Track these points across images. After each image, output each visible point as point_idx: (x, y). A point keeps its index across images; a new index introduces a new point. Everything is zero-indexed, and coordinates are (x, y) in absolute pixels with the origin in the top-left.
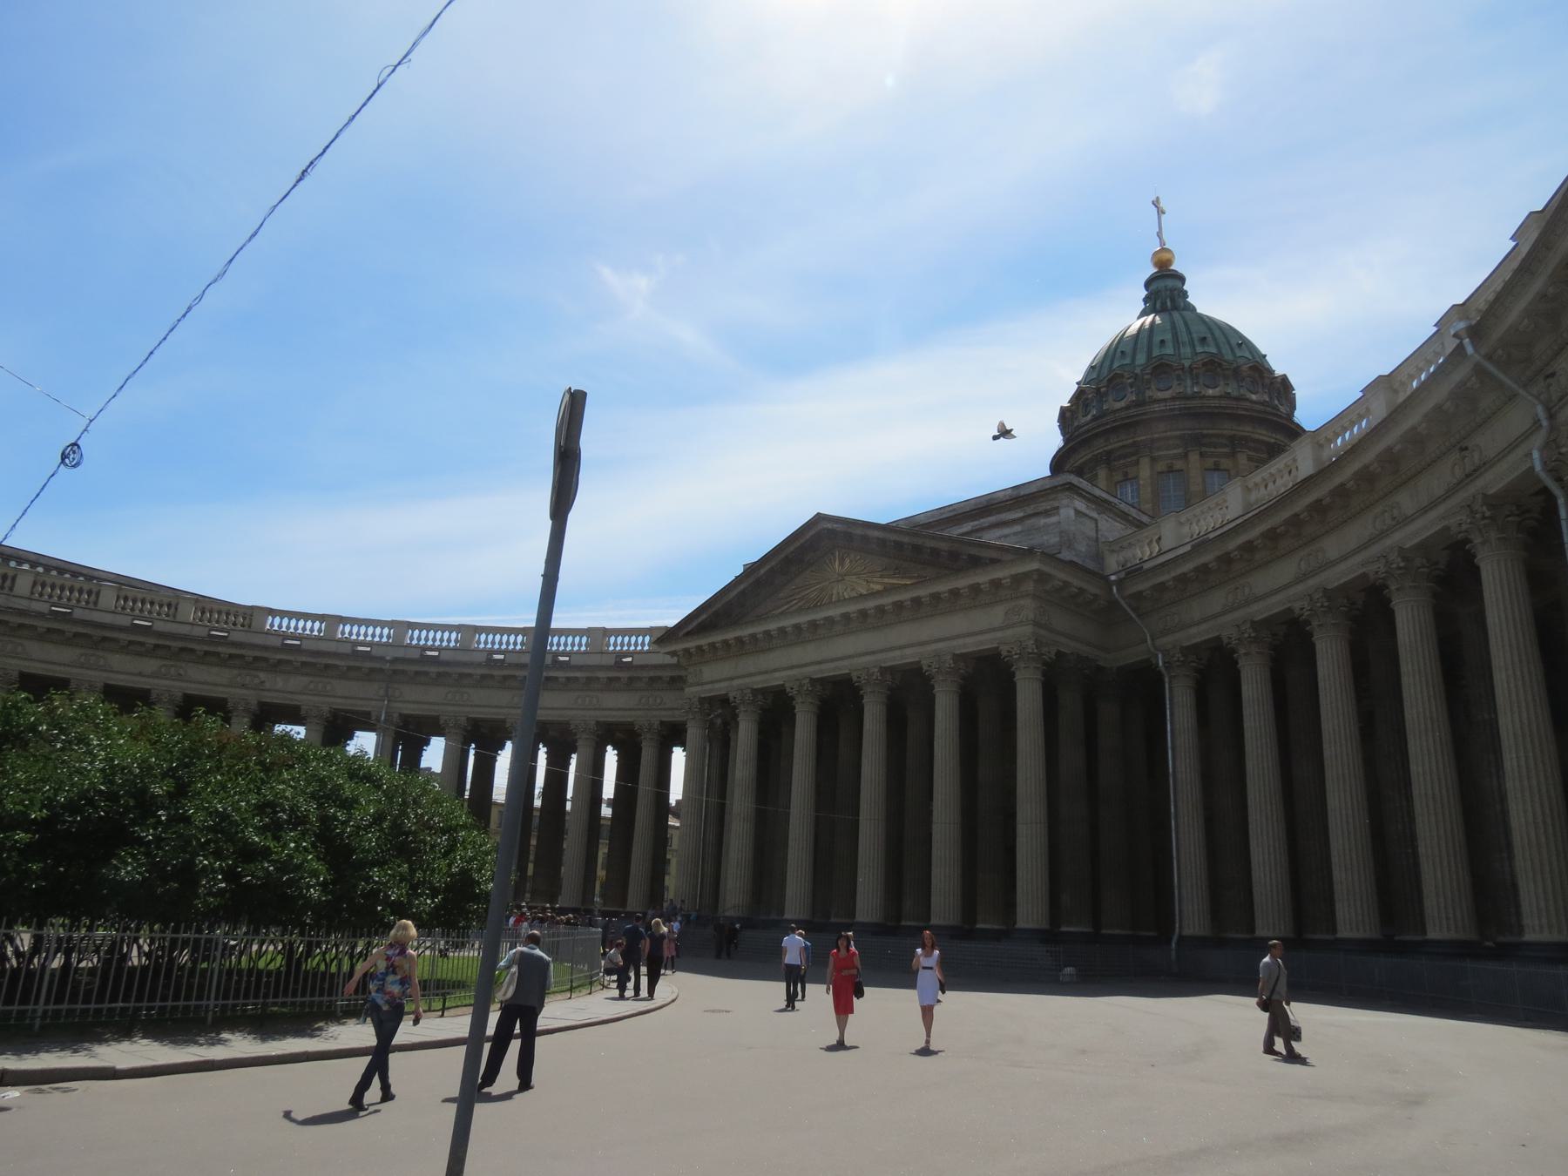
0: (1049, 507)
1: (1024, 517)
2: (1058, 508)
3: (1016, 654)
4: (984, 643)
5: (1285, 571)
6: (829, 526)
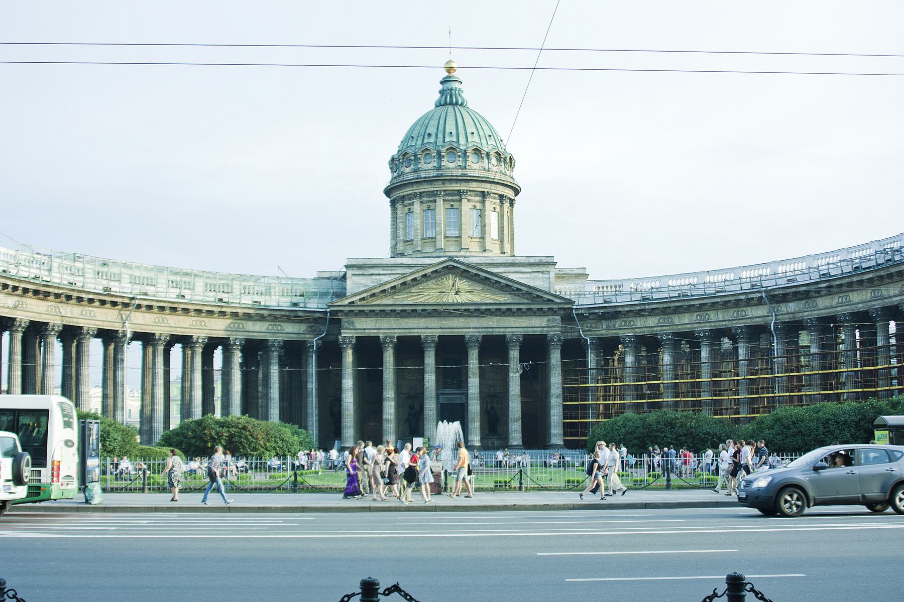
0: (545, 270)
1: (532, 272)
2: (549, 272)
3: (555, 339)
4: (538, 331)
5: (652, 321)
6: (455, 265)
